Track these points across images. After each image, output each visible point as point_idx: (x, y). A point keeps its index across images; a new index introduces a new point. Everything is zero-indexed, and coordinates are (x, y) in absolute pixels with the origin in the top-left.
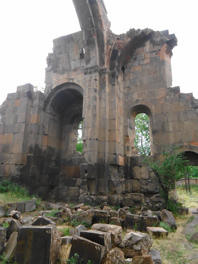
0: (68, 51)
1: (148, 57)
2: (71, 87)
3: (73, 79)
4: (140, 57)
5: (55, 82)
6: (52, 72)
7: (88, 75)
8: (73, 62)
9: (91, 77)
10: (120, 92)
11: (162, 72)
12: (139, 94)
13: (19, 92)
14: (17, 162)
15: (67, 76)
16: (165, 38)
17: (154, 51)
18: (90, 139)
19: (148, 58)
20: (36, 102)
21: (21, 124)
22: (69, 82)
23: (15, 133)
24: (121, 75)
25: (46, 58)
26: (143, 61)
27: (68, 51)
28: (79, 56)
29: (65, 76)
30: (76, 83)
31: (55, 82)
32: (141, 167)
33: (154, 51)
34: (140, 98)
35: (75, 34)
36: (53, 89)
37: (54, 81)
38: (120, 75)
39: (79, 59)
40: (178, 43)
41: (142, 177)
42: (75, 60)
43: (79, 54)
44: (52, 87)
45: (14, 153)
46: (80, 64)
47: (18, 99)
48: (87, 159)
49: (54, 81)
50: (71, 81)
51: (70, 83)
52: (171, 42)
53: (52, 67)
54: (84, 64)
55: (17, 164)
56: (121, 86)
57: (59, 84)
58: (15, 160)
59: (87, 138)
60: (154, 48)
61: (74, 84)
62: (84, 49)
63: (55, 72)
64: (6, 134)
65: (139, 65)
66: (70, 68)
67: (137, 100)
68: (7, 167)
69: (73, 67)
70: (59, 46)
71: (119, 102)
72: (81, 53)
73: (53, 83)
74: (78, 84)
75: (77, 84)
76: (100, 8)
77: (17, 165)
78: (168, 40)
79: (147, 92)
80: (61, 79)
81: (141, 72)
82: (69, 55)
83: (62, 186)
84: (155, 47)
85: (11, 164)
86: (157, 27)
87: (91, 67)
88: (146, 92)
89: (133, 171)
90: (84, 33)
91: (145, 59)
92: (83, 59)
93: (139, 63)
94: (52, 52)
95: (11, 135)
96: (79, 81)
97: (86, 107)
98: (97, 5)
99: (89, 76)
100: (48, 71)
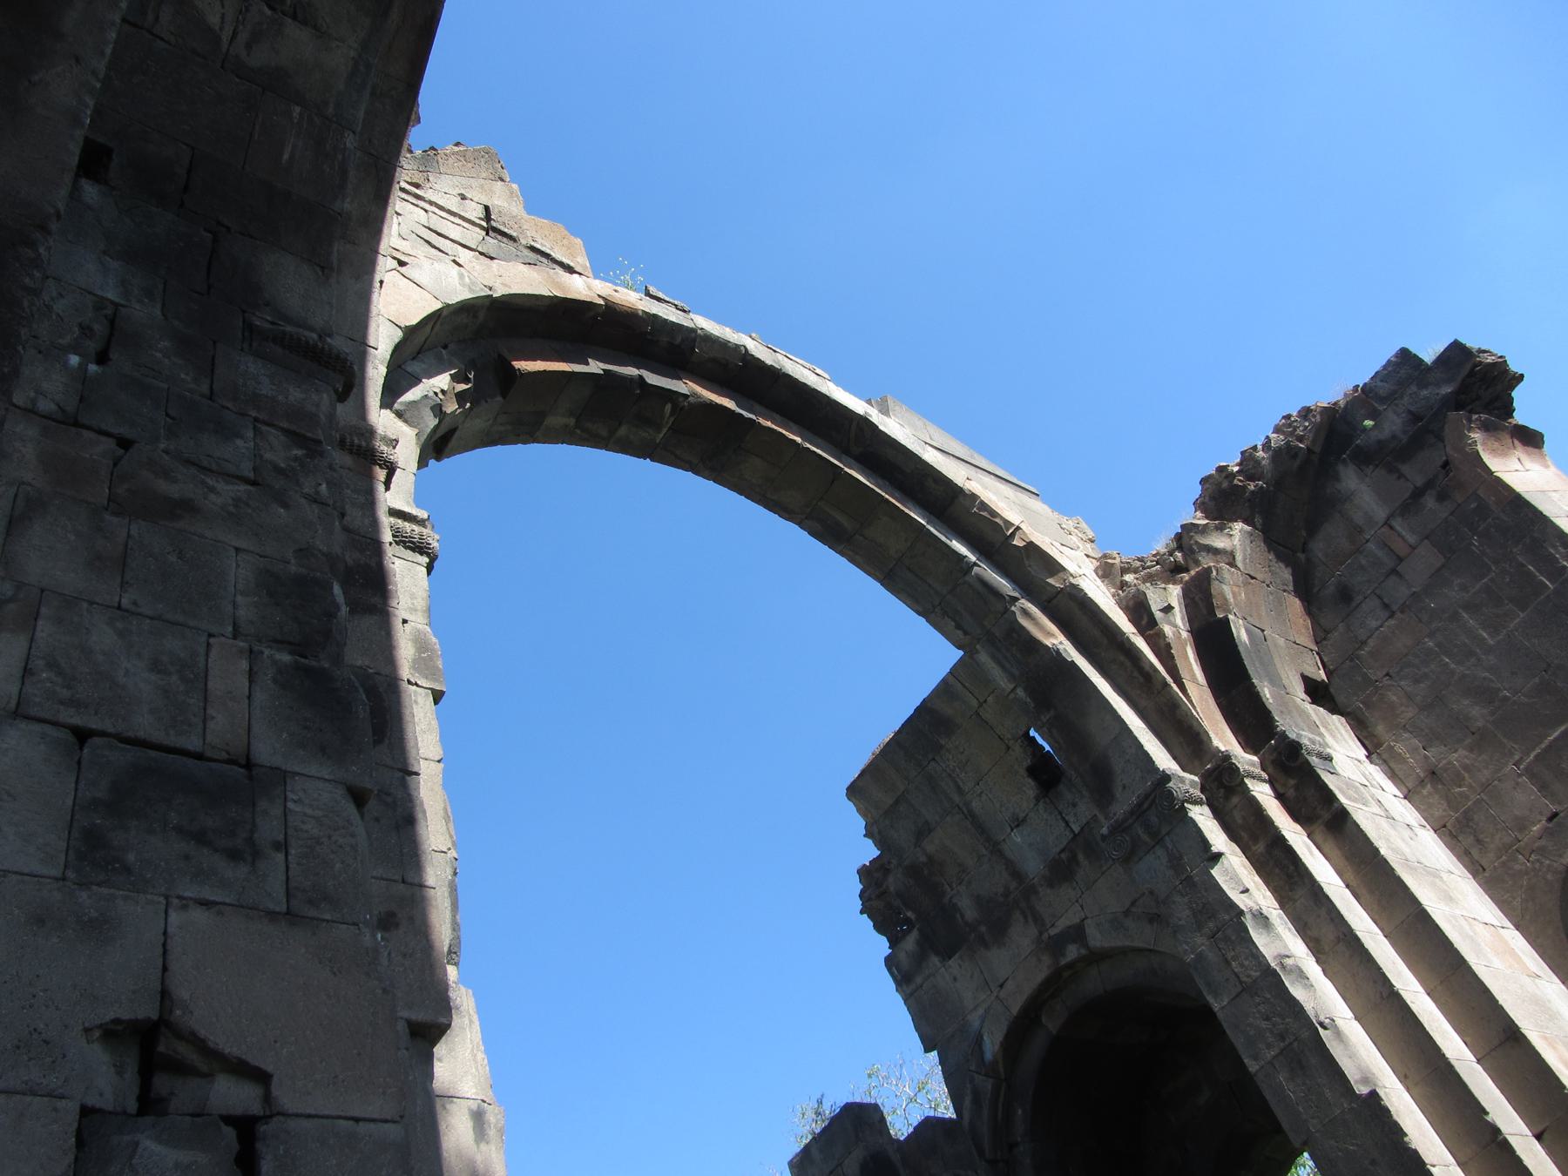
0: (956, 798)
1: (1412, 539)
2: (1094, 983)
3: (1077, 933)
5: (987, 1011)
6: (935, 960)
8: (1017, 837)
10: (1407, 833)
15: (1033, 931)
16: (1425, 392)
17: (1418, 494)
19: (1413, 548)
22: (1063, 962)
24: (1334, 737)
25: (858, 904)
27: (956, 798)
28: (1030, 788)
29: (1022, 937)
30: (1106, 945)
31: (981, 1011)
33: (1418, 494)
35: (945, 689)
38: (1329, 740)
39: (1037, 800)
40: (1514, 366)
42: (1022, 815)
43: (1023, 772)
49: (975, 1008)
50: (1072, 952)
51: (1070, 966)
52: (1476, 388)
53: (914, 935)
54: (1084, 810)
56: (1379, 794)
57: (1015, 1010)
60: (1401, 476)
62: (1032, 733)
63: (947, 954)
66: (1017, 875)
69: (1033, 866)
70: (897, 802)
71: (1449, 899)
72: (1028, 762)
73: (974, 1020)
74: (1127, 943)
75: (1119, 944)
76: (994, 498)
78: (1447, 389)
80: (1010, 972)
81: (1439, 645)
82: (971, 816)
84: (1405, 468)
86: (1334, 374)
87: (1140, 805)
90: (984, 657)
91: (1400, 560)
92: (1061, 787)
93: (1386, 606)
94: (869, 852)
97: (1271, 1063)
98: (974, 497)
100: (903, 973)
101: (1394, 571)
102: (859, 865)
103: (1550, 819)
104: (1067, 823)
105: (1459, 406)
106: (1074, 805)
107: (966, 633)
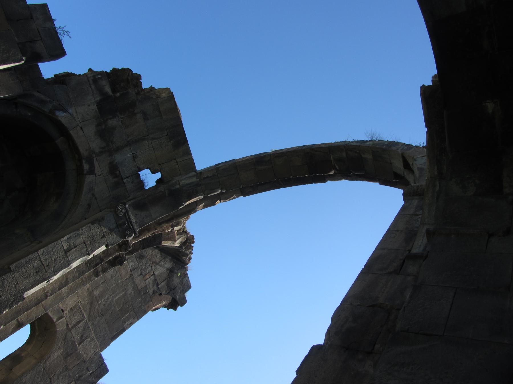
0: (151, 136)
6: (98, 99)
8: (130, 155)
13: (32, 18)
16: (179, 291)
22: (84, 161)
27: (151, 136)
29: (96, 144)
30: (86, 182)
31: (75, 115)
42: (136, 159)
44: (60, 110)
46: (128, 175)
50: (86, 167)
53: (111, 93)
57: (71, 132)
61: (80, 174)
63: (99, 105)
66: (118, 149)
73: (72, 110)
86: (194, 270)
90: (194, 180)
94: (145, 85)
102: (143, 77)
103: (62, 310)
104: (127, 177)
105: (173, 298)
106: (132, 182)
107: (205, 178)
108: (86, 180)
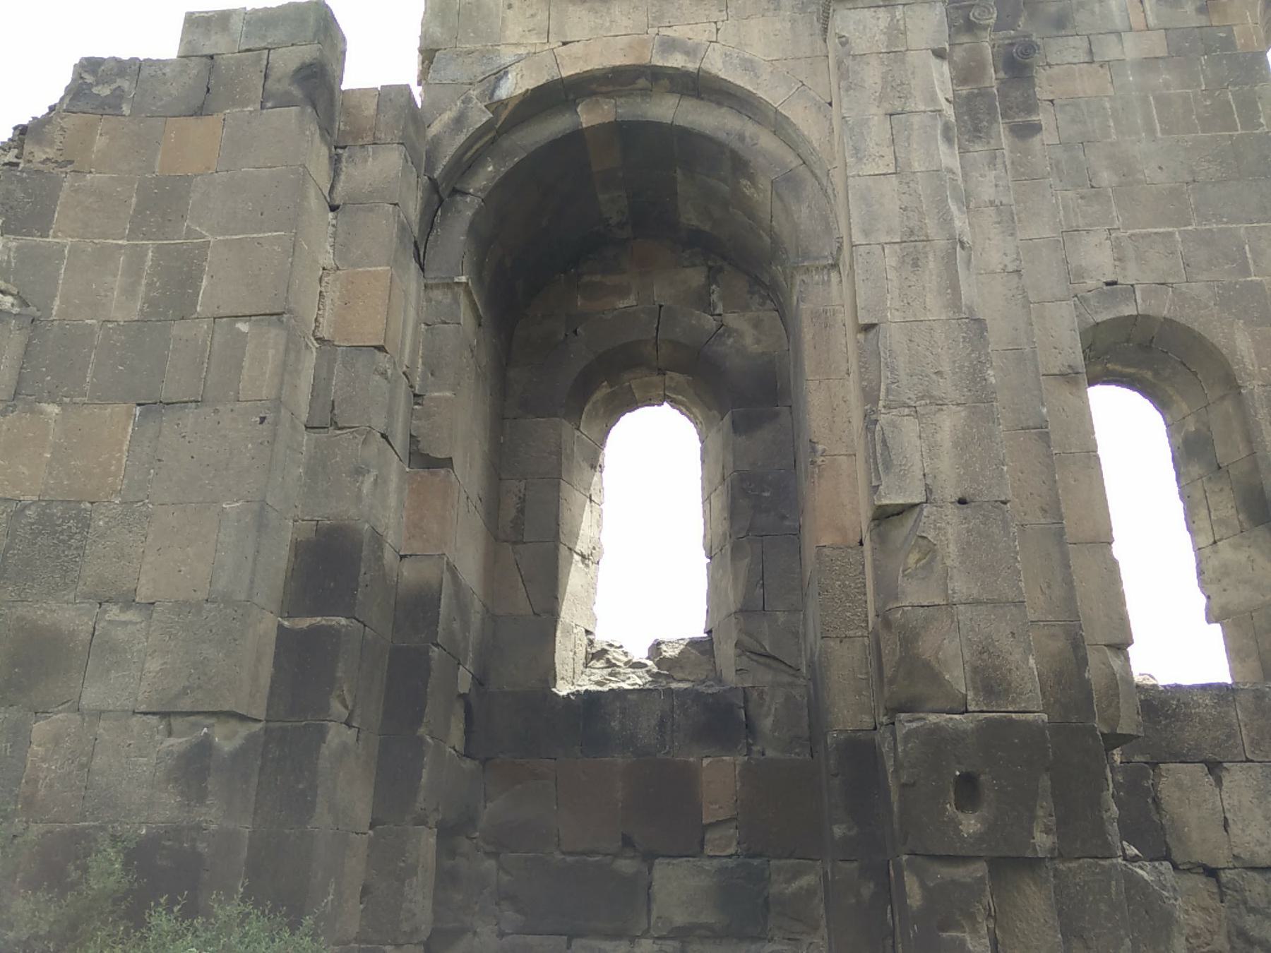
3: (690, 52)
4: (1093, 13)
7: (868, 13)
9: (896, 32)
11: (1262, 120)
12: (1117, 246)
14: (184, 692)
18: (962, 502)
20: (383, 167)
21: (243, 327)
23: (154, 407)
26: (1121, 40)
31: (522, 51)
32: (1214, 767)
34: (1131, 275)
36: (503, 103)
37: (517, 45)
41: (1236, 851)
45: (143, 595)
47: (200, 111)
48: (957, 678)
49: (517, 45)
50: (677, 61)
55: (185, 704)
57: (566, 72)
58: (153, 665)
59: (929, 490)
61: (697, 86)
64: (53, 409)
65: (1092, 62)
67: (1114, 283)
68: (57, 740)
77: (177, 723)
79: (1177, 235)
83: (502, 935)
85: (100, 714)
88: (1171, 234)
89: (1156, 801)
95: (119, 421)
96: (749, 66)
99: (883, 24)
101: (1118, 33)
103: (1108, 284)
108: (714, 71)
